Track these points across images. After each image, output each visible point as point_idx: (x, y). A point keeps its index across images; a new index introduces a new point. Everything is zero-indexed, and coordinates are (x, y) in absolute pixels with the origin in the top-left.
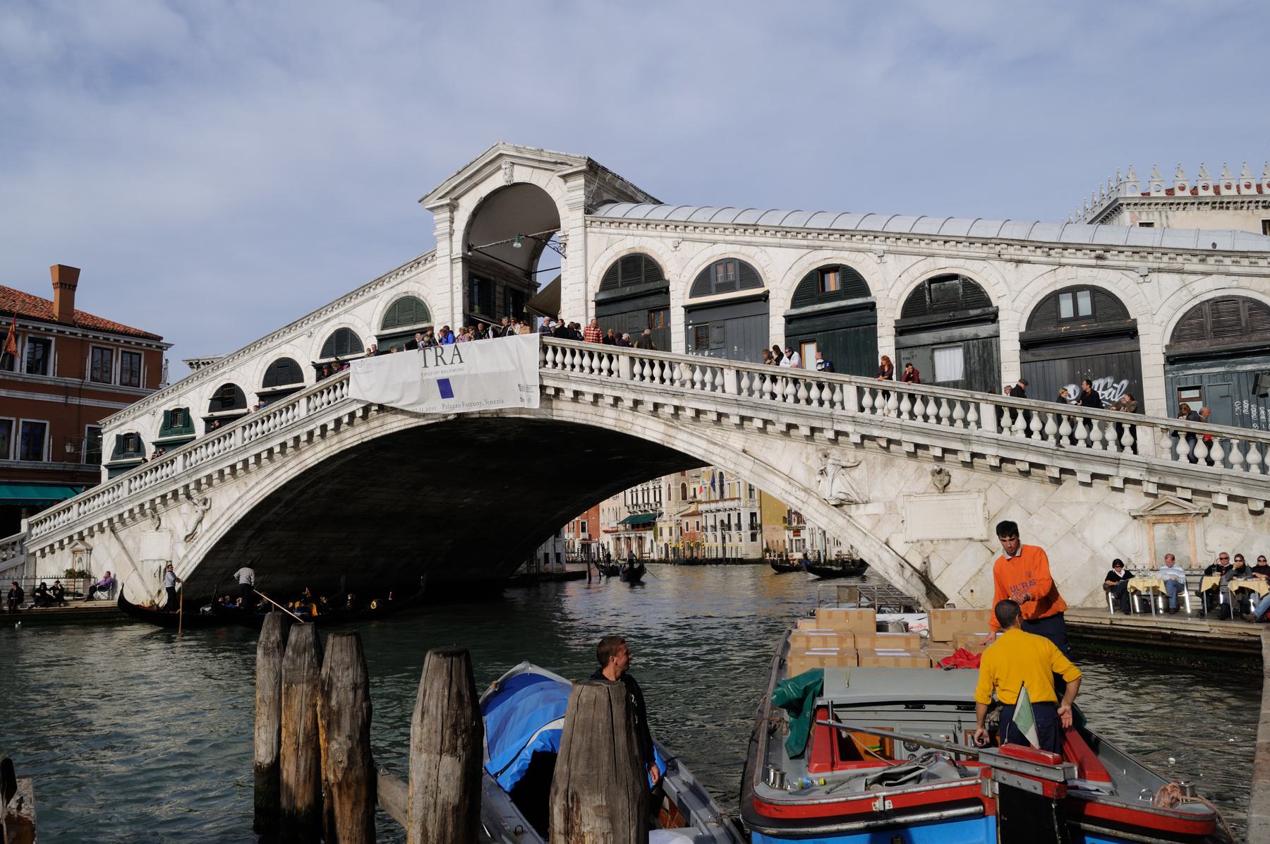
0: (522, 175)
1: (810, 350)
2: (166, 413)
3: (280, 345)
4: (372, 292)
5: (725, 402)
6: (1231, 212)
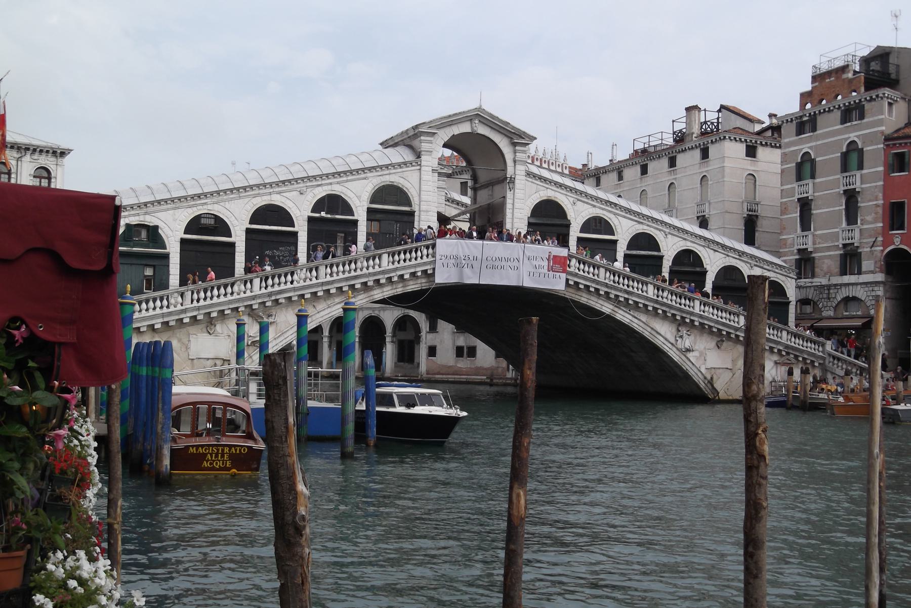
0: (482, 130)
3: (270, 194)
4: (363, 176)
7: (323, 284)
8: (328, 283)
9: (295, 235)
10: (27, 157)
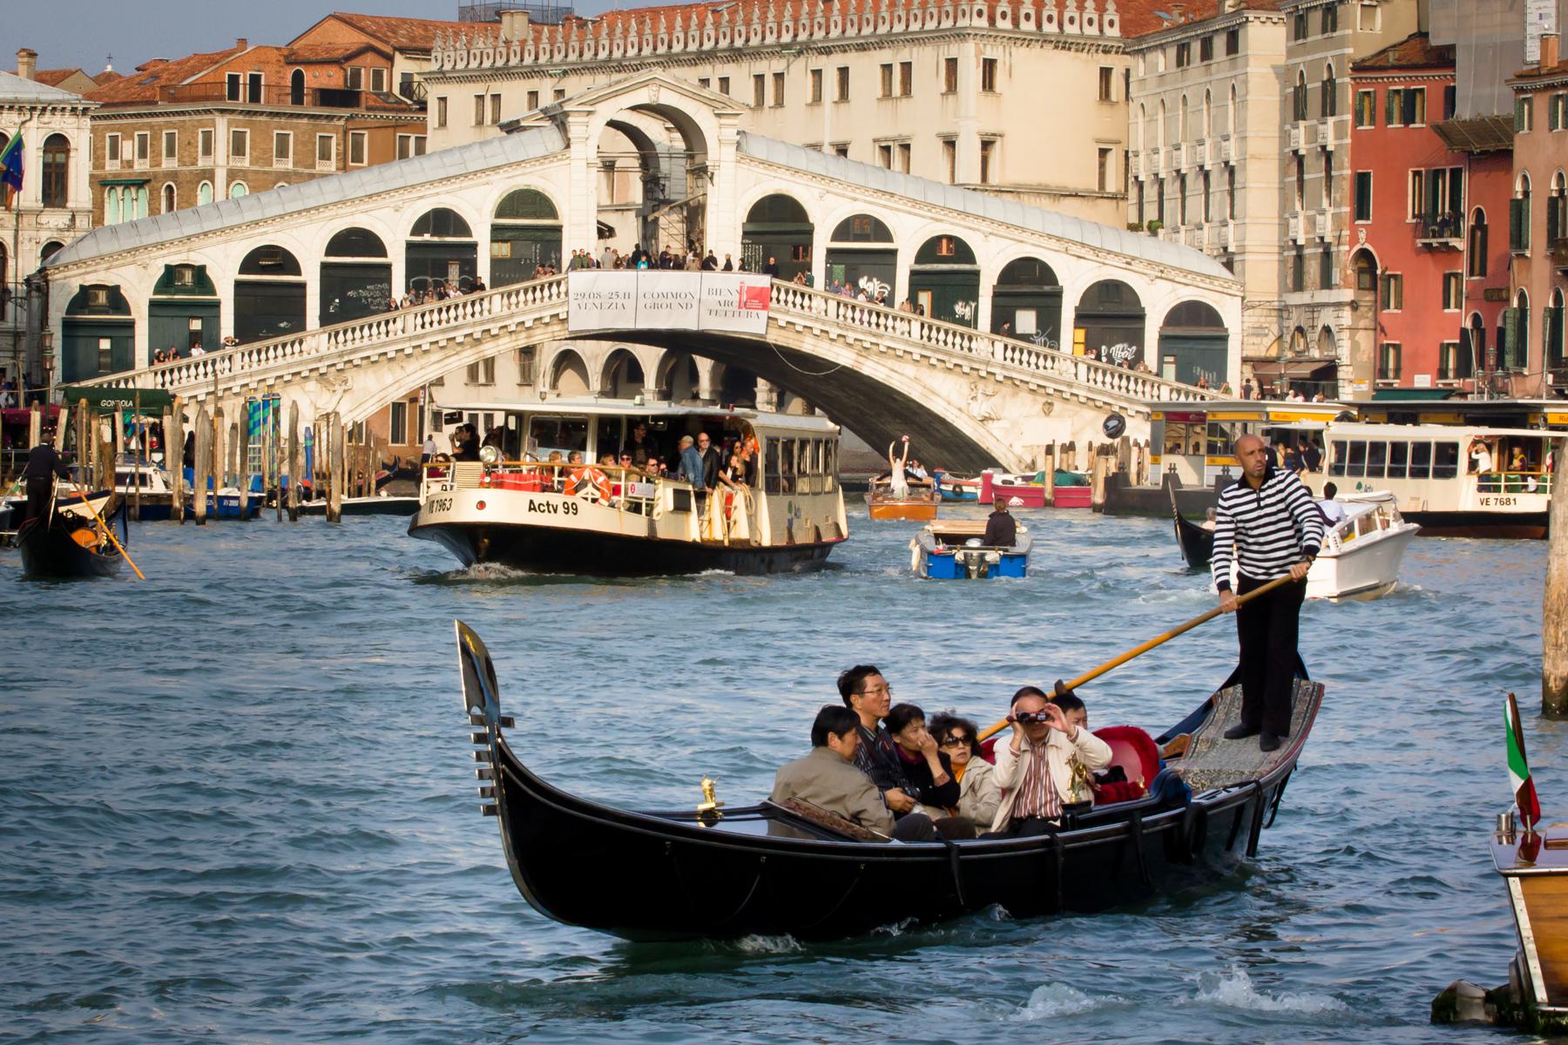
1: (925, 299)
2: (168, 267)
3: (352, 214)
5: (915, 344)
6: (1072, 53)
7: (410, 339)
8: (418, 337)
9: (388, 267)
10: (34, 123)
